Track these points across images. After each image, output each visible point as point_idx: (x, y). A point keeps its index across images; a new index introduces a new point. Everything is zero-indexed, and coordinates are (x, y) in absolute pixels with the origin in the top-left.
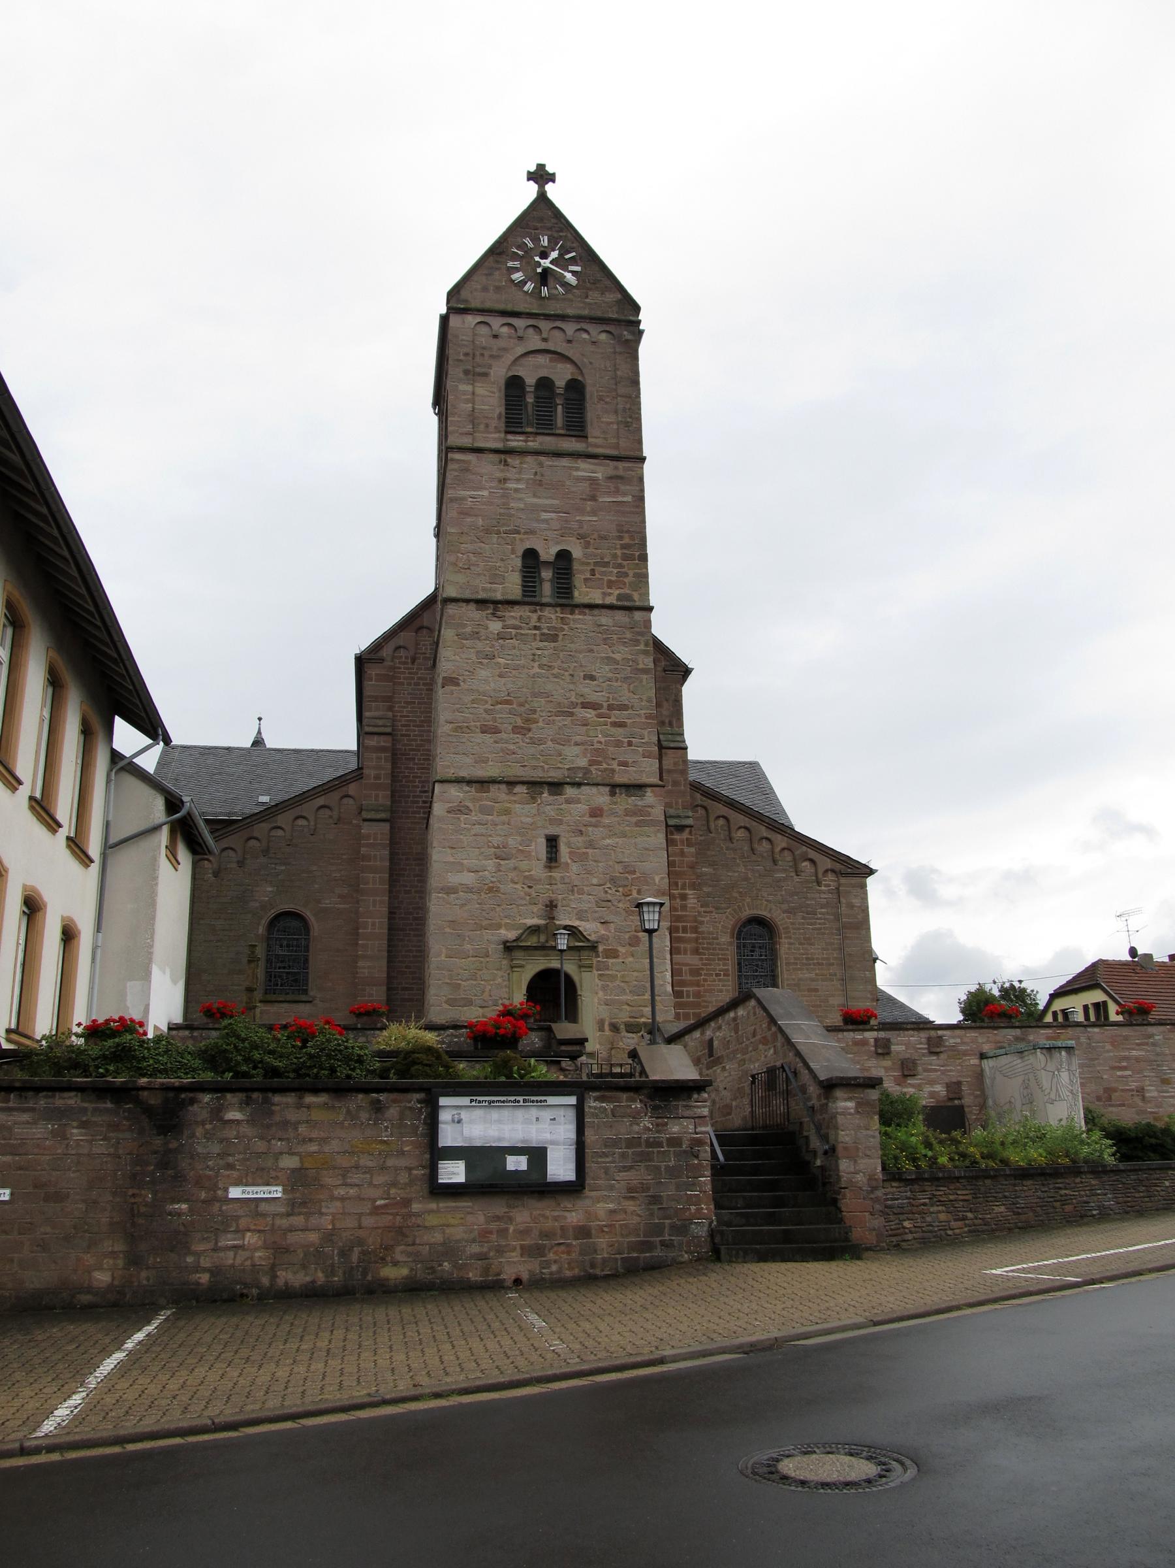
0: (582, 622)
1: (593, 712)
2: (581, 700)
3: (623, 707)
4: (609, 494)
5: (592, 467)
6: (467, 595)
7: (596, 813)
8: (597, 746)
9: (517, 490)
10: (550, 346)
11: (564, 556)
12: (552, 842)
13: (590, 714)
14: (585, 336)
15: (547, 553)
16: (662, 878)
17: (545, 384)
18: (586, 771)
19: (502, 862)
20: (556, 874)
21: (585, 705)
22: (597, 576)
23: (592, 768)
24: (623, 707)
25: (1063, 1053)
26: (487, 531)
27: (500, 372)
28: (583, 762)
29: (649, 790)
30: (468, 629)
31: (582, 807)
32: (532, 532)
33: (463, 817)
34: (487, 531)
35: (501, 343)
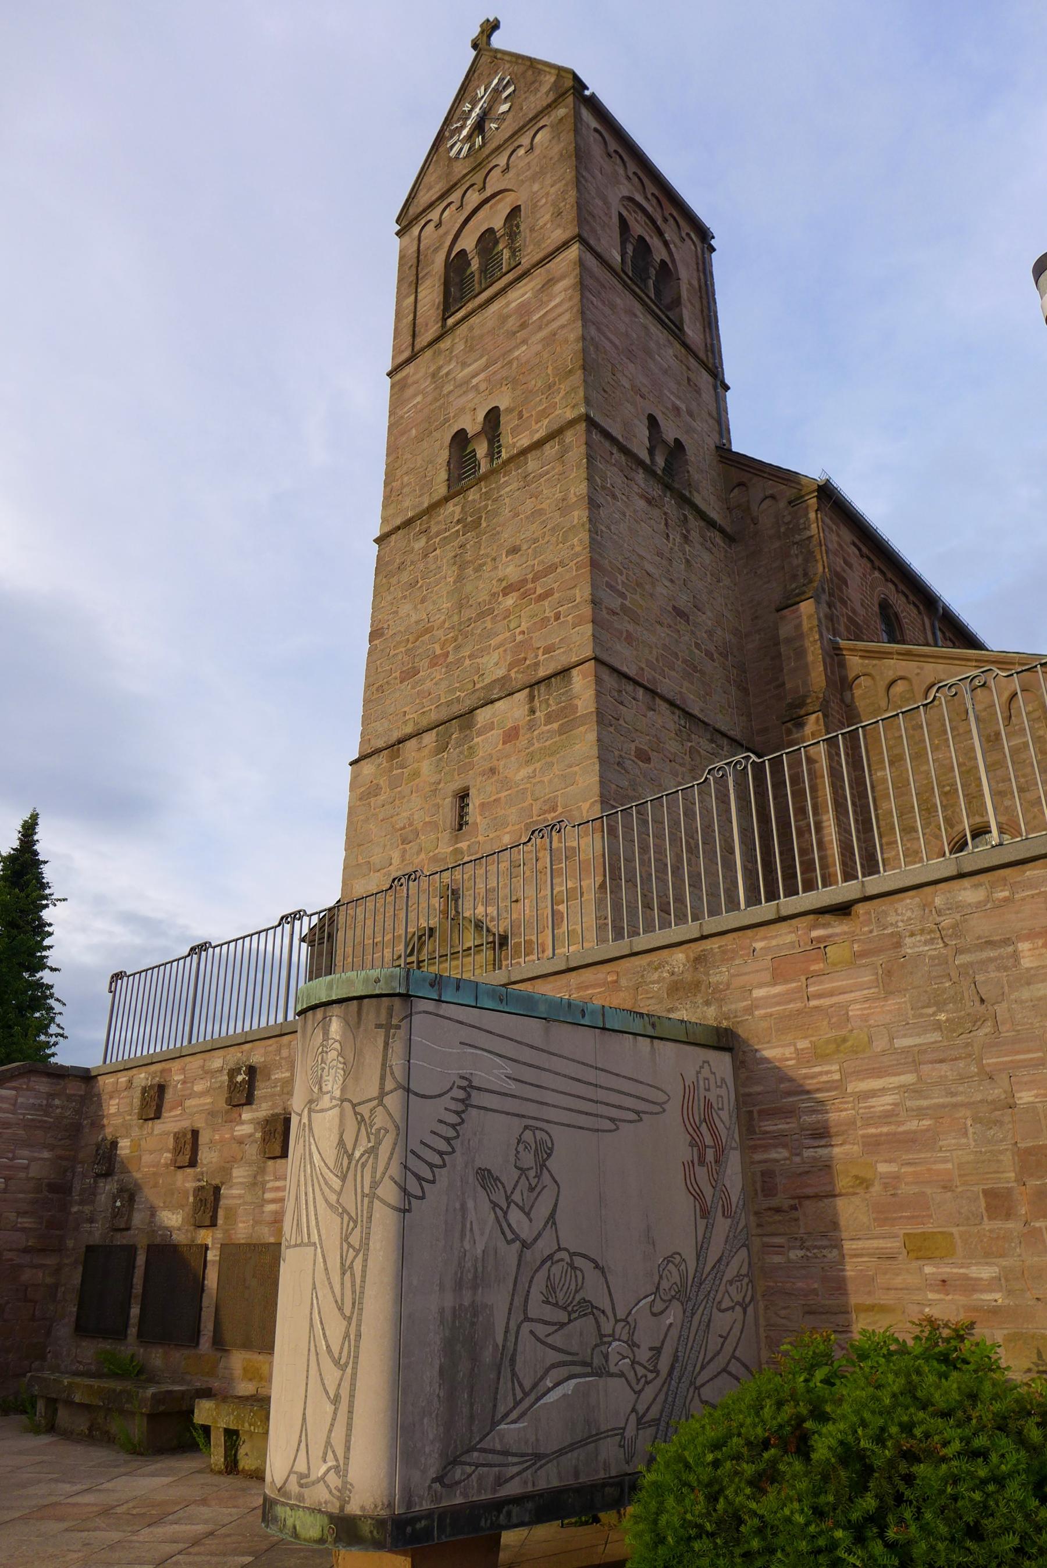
0: (509, 485)
1: (515, 594)
2: (504, 584)
3: (552, 568)
4: (538, 309)
5: (521, 291)
6: (398, 522)
7: (511, 735)
8: (519, 638)
9: (447, 374)
10: (488, 193)
11: (493, 417)
12: (463, 796)
13: (510, 601)
14: (521, 152)
15: (472, 424)
16: (592, 804)
17: (488, 238)
18: (505, 679)
19: (407, 847)
20: (463, 845)
21: (506, 592)
22: (526, 415)
23: (513, 674)
24: (552, 568)
25: (335, 1027)
26: (419, 439)
27: (438, 263)
28: (500, 673)
29: (575, 672)
30: (396, 565)
31: (496, 734)
32: (462, 410)
33: (373, 800)
34: (419, 439)
35: (441, 231)
